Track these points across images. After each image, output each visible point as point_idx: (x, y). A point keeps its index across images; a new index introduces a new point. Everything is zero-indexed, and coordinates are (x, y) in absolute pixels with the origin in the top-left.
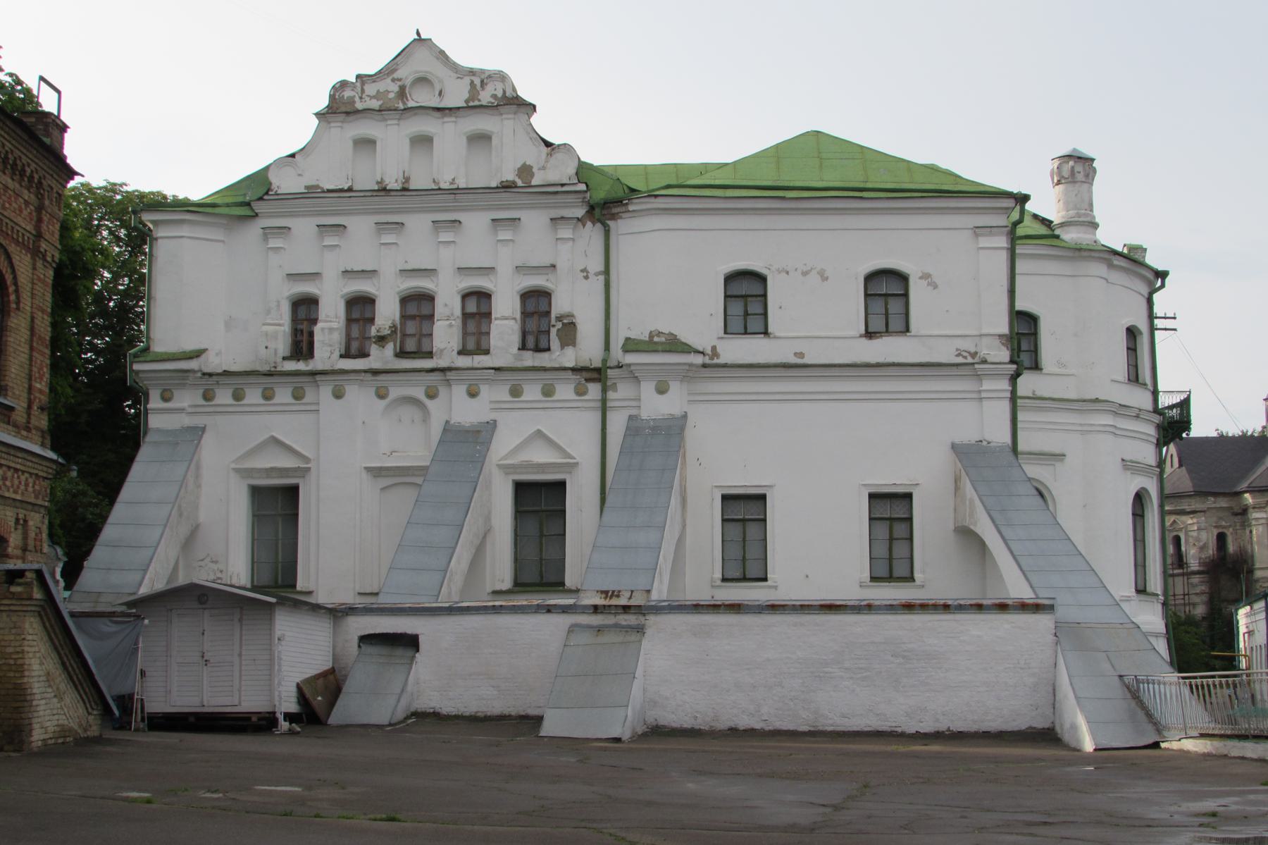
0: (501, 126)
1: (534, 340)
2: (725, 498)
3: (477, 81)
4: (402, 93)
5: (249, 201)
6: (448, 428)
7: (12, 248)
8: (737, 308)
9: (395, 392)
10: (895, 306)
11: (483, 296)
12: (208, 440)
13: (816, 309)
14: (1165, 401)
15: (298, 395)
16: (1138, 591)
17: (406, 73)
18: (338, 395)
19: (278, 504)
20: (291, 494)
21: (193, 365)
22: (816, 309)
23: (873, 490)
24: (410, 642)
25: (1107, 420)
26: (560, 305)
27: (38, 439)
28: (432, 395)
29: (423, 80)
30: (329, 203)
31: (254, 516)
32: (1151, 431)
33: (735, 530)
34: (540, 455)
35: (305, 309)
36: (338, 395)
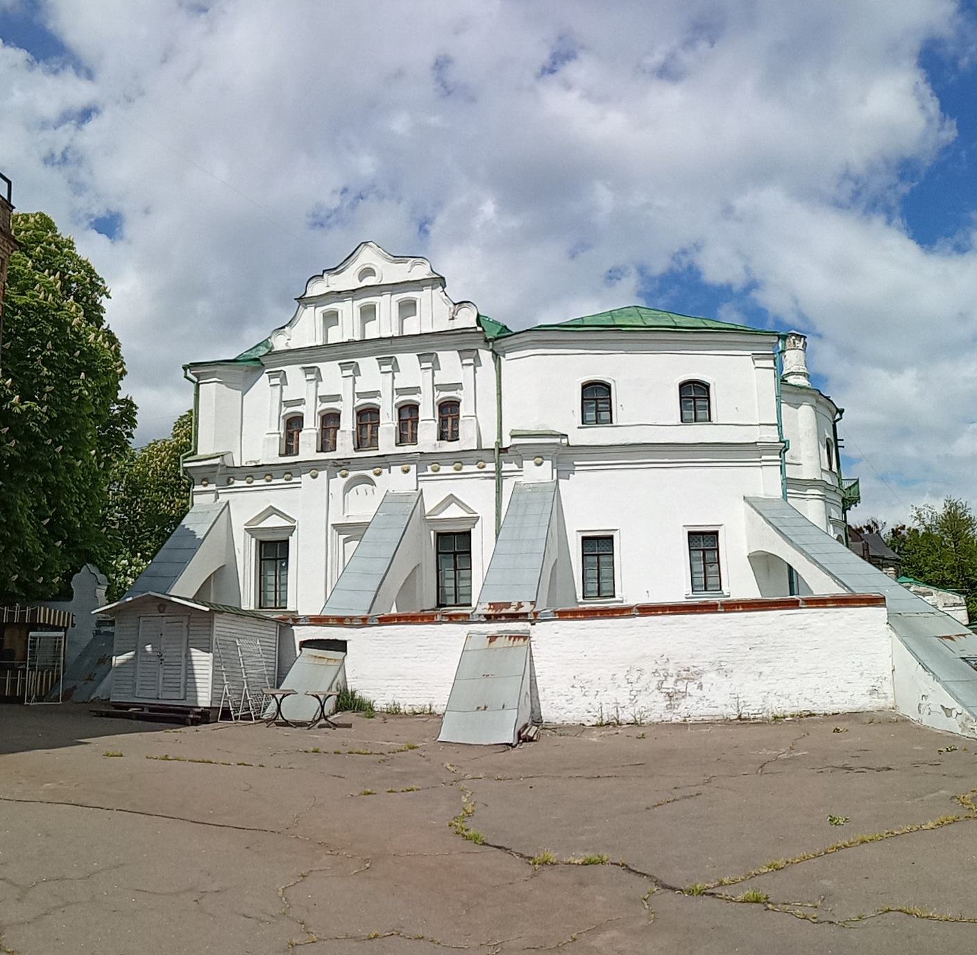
11: (414, 408)
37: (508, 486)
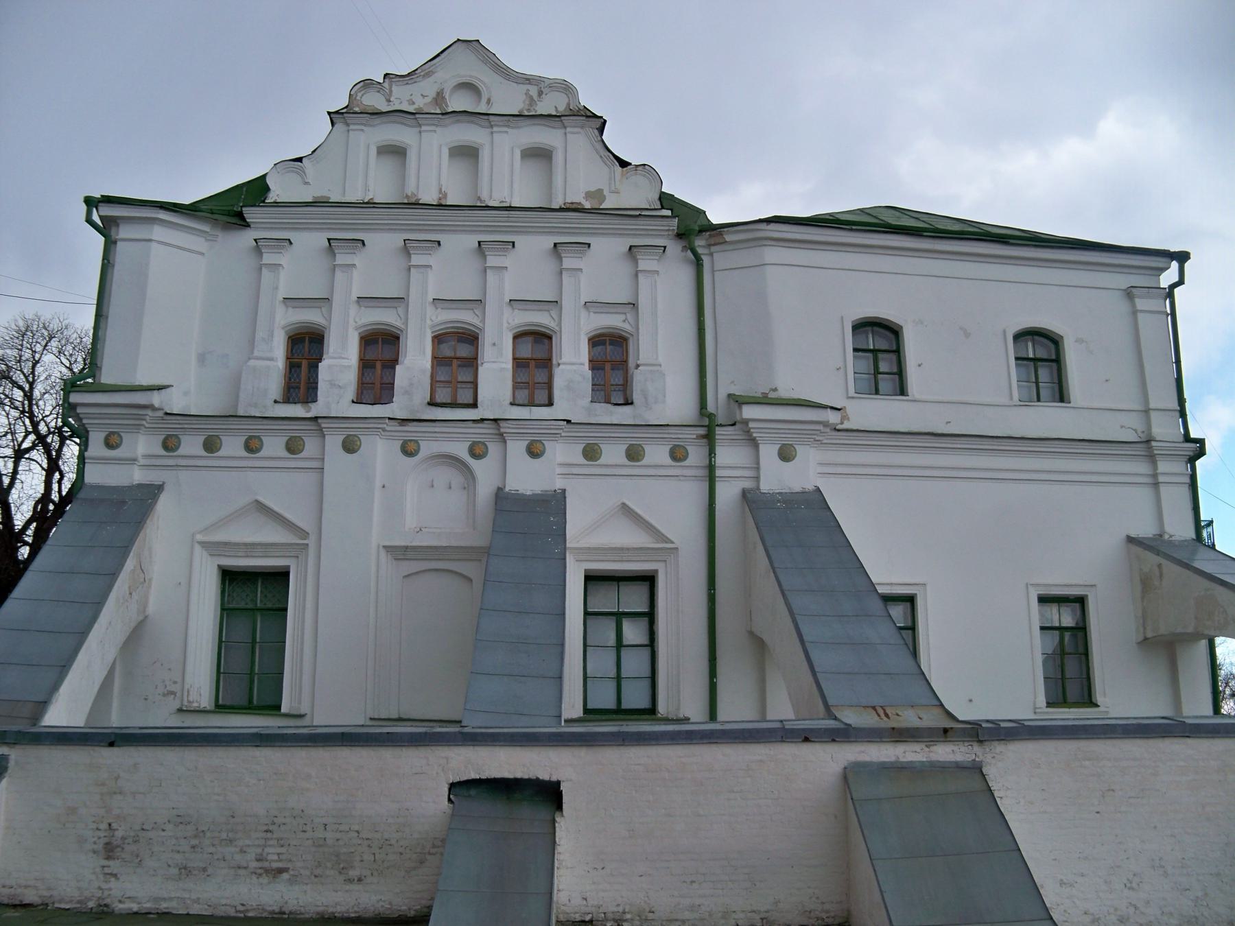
3: (534, 91)
4: (439, 98)
6: (500, 495)
9: (428, 448)
12: (164, 504)
13: (962, 370)
15: (293, 447)
17: (446, 76)
18: (350, 446)
19: (255, 595)
20: (280, 577)
21: (156, 399)
22: (962, 370)
23: (1043, 592)
24: (549, 794)
28: (477, 452)
29: (469, 87)
30: (343, 221)
31: (223, 609)
34: (626, 536)
36: (350, 446)
37: (727, 493)
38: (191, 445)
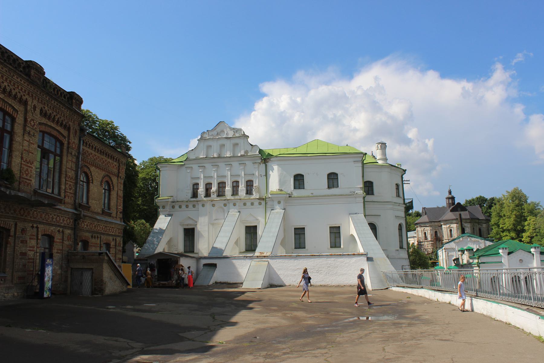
0: (241, 141)
1: (249, 192)
2: (295, 229)
4: (218, 134)
5: (187, 161)
7: (111, 176)
8: (297, 183)
10: (335, 181)
11: (237, 182)
14: (407, 201)
15: (194, 206)
16: (400, 248)
17: (219, 129)
18: (203, 205)
22: (316, 182)
24: (214, 266)
25: (391, 206)
26: (256, 184)
27: (119, 219)
32: (402, 208)
33: (298, 236)
35: (195, 187)
36: (203, 205)
38: (177, 207)
